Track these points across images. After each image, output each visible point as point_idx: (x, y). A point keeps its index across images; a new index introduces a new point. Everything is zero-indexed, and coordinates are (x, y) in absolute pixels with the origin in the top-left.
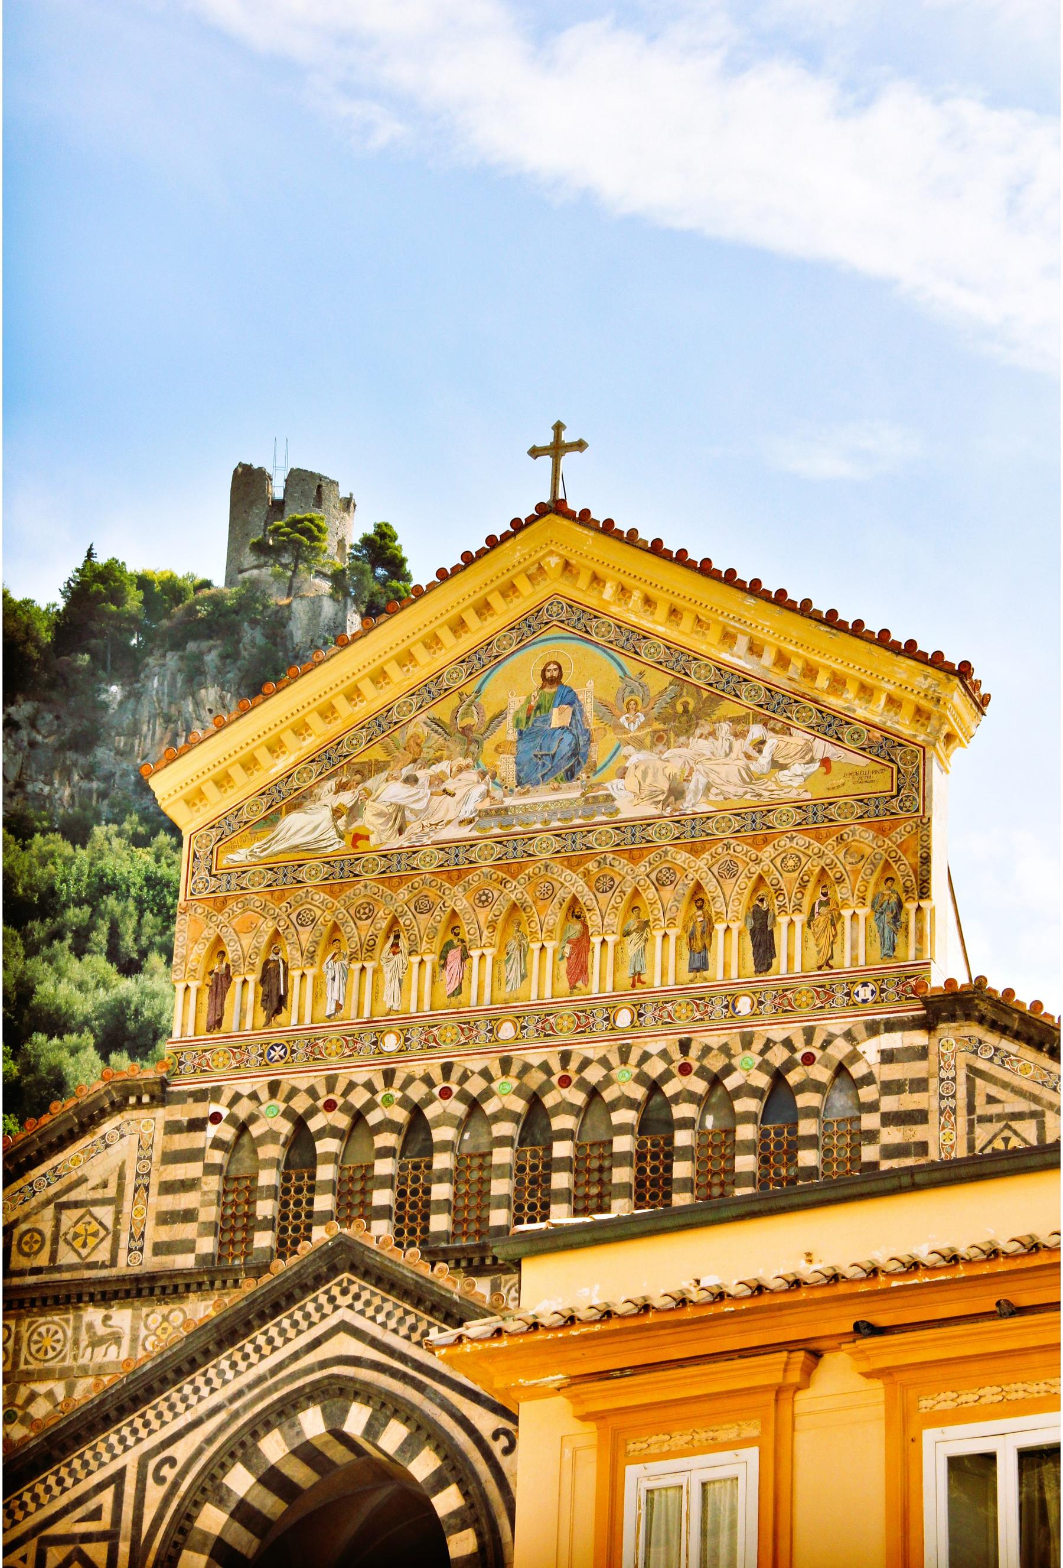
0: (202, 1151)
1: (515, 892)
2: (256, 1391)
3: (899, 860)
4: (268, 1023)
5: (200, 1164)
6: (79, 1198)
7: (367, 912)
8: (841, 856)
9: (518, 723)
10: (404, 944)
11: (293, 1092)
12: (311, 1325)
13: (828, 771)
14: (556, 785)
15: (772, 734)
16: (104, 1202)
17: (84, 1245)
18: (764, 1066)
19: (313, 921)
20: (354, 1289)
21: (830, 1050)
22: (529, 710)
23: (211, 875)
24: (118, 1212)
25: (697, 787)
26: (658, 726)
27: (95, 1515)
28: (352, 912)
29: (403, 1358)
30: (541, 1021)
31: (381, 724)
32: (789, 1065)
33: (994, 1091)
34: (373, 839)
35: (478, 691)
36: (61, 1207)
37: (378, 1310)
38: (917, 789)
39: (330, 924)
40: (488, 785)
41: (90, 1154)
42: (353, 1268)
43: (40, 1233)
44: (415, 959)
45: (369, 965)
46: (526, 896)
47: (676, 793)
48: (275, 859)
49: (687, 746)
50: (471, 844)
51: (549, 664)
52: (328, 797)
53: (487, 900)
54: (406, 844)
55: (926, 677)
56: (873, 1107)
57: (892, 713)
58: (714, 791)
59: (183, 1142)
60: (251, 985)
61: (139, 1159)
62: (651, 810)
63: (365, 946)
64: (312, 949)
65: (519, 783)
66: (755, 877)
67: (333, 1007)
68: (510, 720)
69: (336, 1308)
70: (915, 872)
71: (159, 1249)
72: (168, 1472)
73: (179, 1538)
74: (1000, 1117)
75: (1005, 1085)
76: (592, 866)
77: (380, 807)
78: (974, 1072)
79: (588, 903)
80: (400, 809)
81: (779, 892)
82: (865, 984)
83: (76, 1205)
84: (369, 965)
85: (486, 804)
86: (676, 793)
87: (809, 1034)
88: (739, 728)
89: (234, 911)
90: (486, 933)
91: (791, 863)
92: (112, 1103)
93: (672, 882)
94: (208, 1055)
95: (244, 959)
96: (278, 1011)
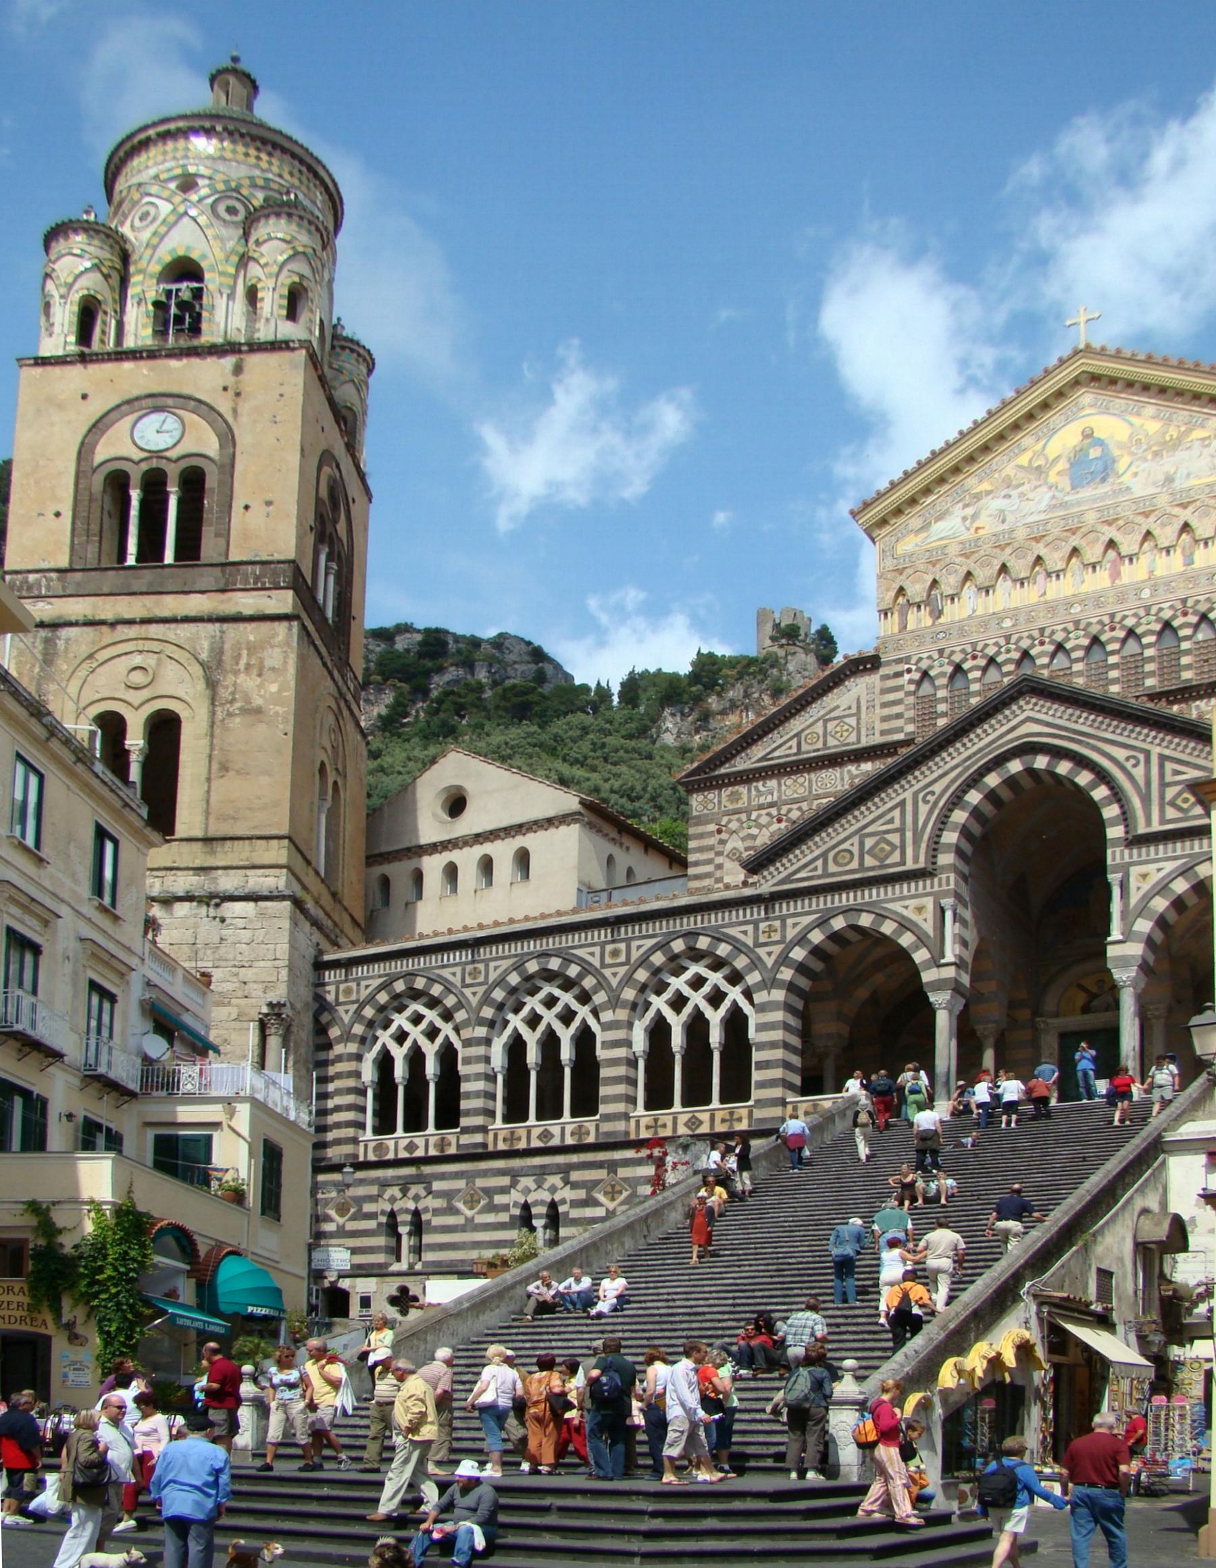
1: (1075, 541)
30: (1097, 599)
47: (1169, 480)
52: (958, 511)
71: (883, 733)
72: (931, 798)
80: (1002, 511)
86: (1169, 480)
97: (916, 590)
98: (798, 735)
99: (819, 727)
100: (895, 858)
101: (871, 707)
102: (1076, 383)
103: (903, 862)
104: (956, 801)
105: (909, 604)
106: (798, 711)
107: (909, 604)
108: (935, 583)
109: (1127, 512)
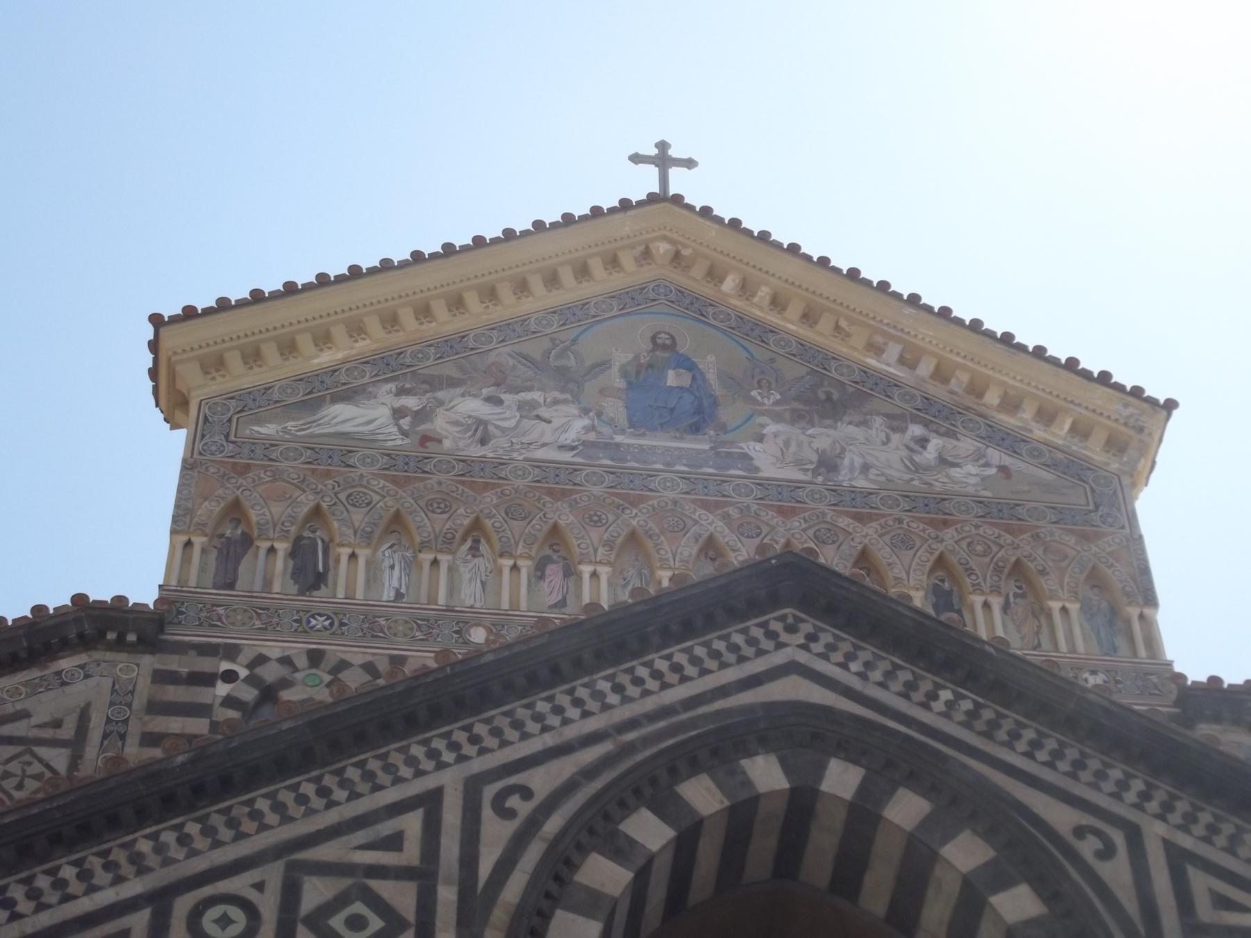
1: (636, 519)
2: (661, 724)
3: (1112, 565)
5: (207, 721)
6: (16, 733)
7: (443, 505)
8: (1040, 551)
9: (624, 374)
10: (484, 547)
11: (343, 665)
14: (678, 435)
15: (934, 435)
17: (20, 787)
19: (368, 504)
20: (807, 628)
23: (227, 440)
25: (852, 463)
26: (796, 405)
27: (394, 842)
28: (422, 503)
31: (452, 345)
34: (447, 444)
35: (575, 341)
37: (850, 657)
38: (1119, 509)
39: (393, 510)
40: (593, 420)
41: (34, 688)
42: (806, 604)
44: (507, 563)
45: (444, 559)
46: (651, 524)
47: (827, 464)
48: (315, 440)
49: (835, 429)
50: (574, 469)
51: (659, 333)
53: (600, 521)
54: (491, 455)
55: (1126, 406)
57: (1076, 440)
58: (873, 471)
59: (175, 693)
60: (281, 555)
61: (112, 704)
62: (799, 476)
63: (441, 538)
64: (368, 529)
65: (632, 425)
66: (937, 553)
67: (392, 594)
68: (615, 369)
69: (780, 646)
70: (1135, 581)
73: (553, 888)
76: (731, 510)
79: (731, 543)
80: (481, 423)
81: (970, 571)
82: (1093, 672)
84: (444, 559)
85: (592, 437)
86: (827, 464)
88: (895, 423)
89: (260, 478)
90: (601, 550)
91: (979, 548)
92: (81, 636)
93: (834, 542)
94: (220, 610)
95: (275, 526)
96: (316, 586)
104: (598, 828)
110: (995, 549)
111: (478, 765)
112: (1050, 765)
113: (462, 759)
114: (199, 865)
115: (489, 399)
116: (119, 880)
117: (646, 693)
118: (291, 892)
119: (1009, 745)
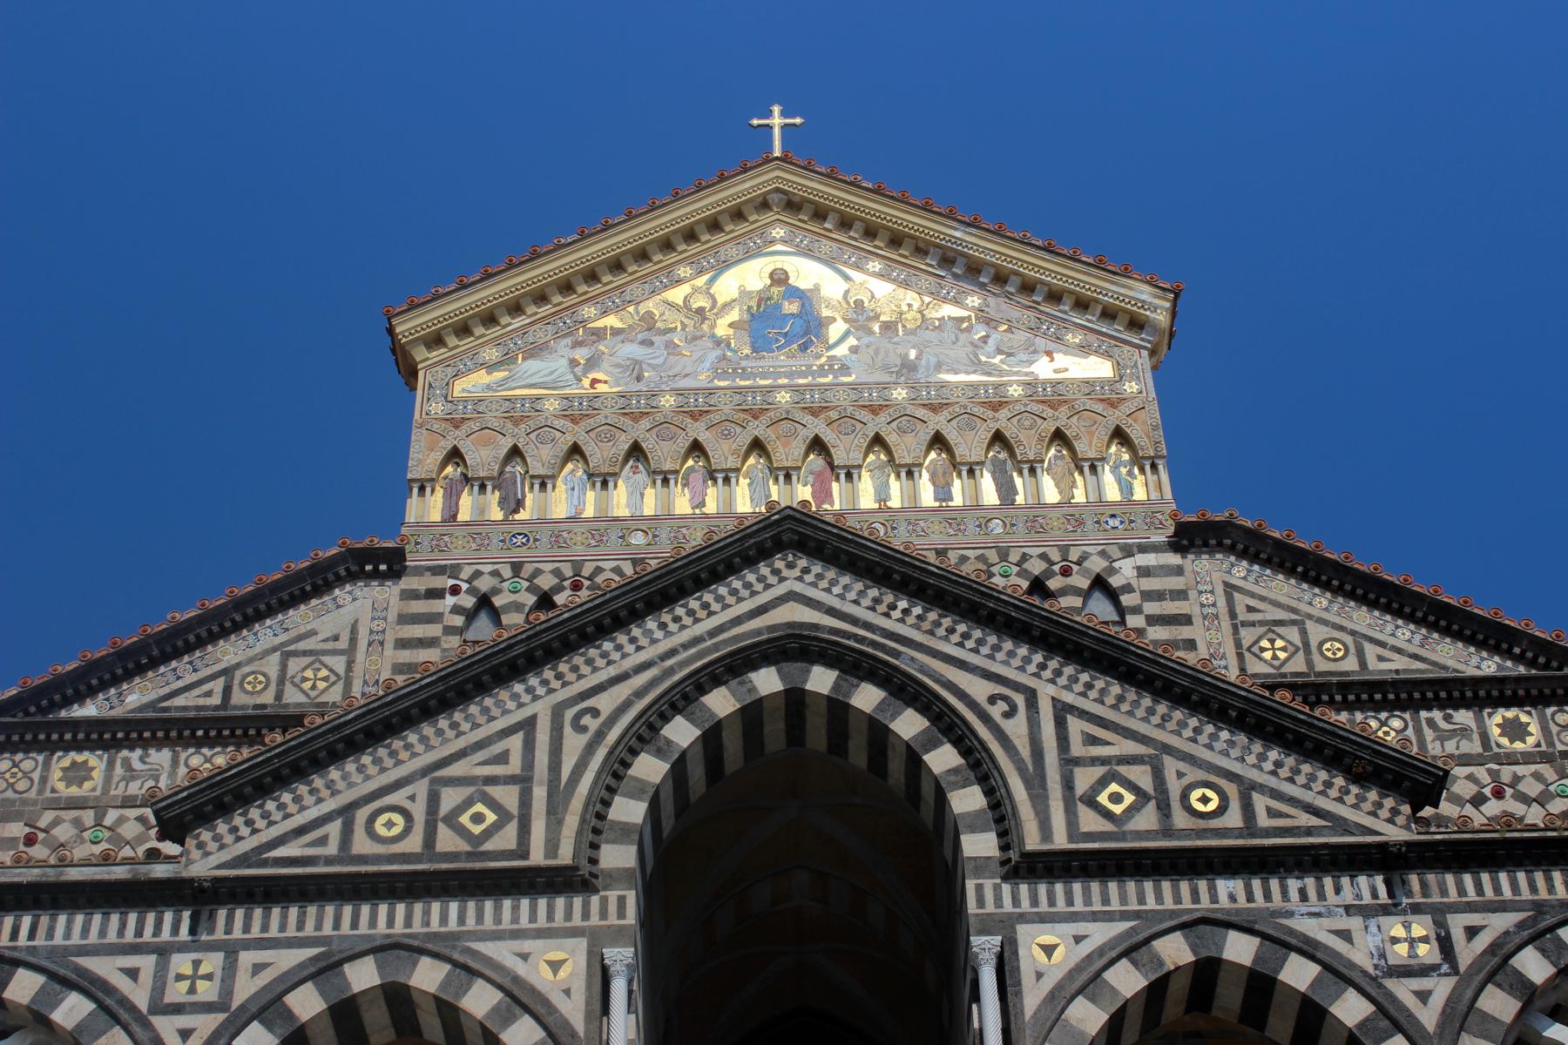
0: (441, 615)
1: (757, 429)
2: (693, 651)
4: (506, 517)
12: (754, 594)
13: (1052, 360)
16: (334, 652)
17: (314, 687)
18: (1023, 573)
21: (1086, 564)
22: (760, 300)
24: (350, 665)
27: (503, 758)
29: (867, 626)
32: (1049, 574)
33: (1252, 602)
36: (287, 656)
43: (264, 675)
50: (710, 392)
56: (1137, 610)
61: (373, 619)
62: (887, 378)
74: (1262, 623)
75: (1263, 599)
77: (615, 360)
78: (1230, 588)
80: (636, 362)
81: (1020, 443)
82: (1113, 516)
83: (305, 653)
87: (1064, 550)
90: (730, 458)
91: (1027, 423)
96: (516, 511)
97: (482, 458)
98: (227, 672)
99: (272, 665)
100: (507, 839)
101: (377, 643)
102: (764, 205)
103: (523, 851)
104: (645, 734)
105: (466, 479)
106: (236, 628)
107: (466, 479)
108: (515, 452)
109: (842, 399)
110: (1039, 421)
111: (562, 695)
112: (976, 651)
113: (551, 691)
114: (372, 786)
115: (642, 343)
116: (320, 801)
117: (683, 627)
118: (434, 800)
119: (946, 638)
